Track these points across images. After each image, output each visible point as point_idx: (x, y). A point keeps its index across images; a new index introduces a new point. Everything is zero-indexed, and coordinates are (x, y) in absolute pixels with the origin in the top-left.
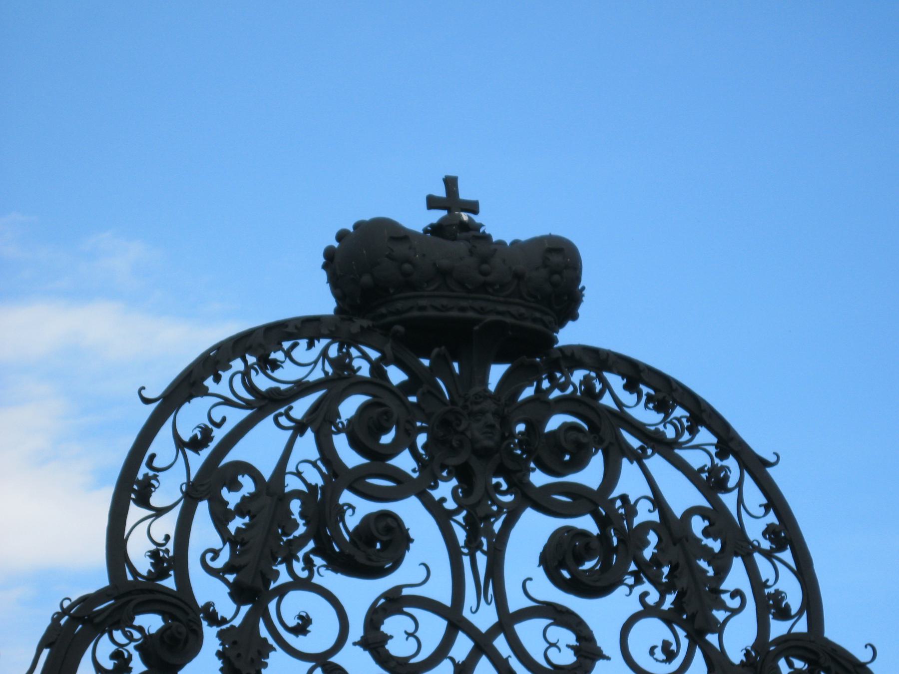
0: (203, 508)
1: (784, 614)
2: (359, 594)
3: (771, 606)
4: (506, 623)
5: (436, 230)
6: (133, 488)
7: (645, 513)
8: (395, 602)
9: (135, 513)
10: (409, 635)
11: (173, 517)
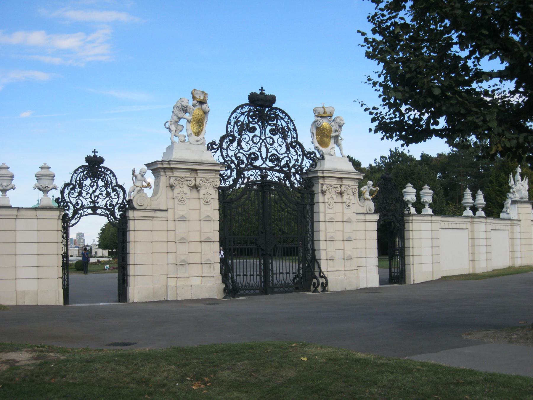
1: (294, 138)
2: (251, 135)
3: (293, 137)
4: (266, 138)
5: (260, 93)
6: (229, 123)
7: (280, 126)
8: (254, 136)
9: (229, 126)
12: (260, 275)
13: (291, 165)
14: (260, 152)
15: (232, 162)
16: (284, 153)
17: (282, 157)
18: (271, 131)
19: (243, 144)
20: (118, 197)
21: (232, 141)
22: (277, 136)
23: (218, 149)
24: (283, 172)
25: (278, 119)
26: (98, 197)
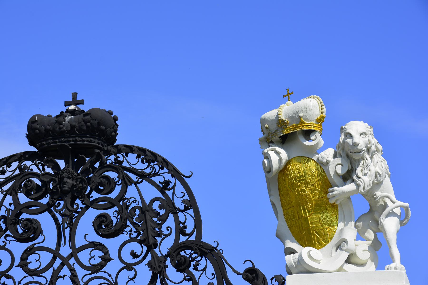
1: (184, 234)
10: (37, 261)
22: (123, 237)
25: (126, 182)
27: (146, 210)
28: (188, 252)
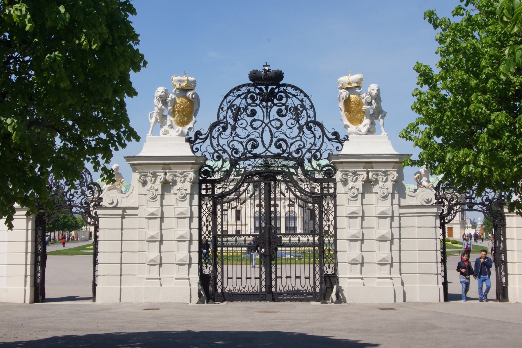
0: (229, 110)
1: (310, 118)
2: (249, 119)
3: (308, 117)
4: (270, 121)
6: (221, 108)
8: (254, 120)
9: (221, 111)
11: (225, 112)
12: (260, 278)
13: (304, 150)
14: (262, 138)
15: (225, 151)
16: (296, 137)
17: (292, 141)
18: (279, 112)
19: (239, 131)
20: (93, 195)
21: (225, 129)
22: (287, 117)
23: (206, 138)
24: (294, 159)
25: (288, 97)
26: (73, 196)
27: (296, 108)
28: (312, 124)
